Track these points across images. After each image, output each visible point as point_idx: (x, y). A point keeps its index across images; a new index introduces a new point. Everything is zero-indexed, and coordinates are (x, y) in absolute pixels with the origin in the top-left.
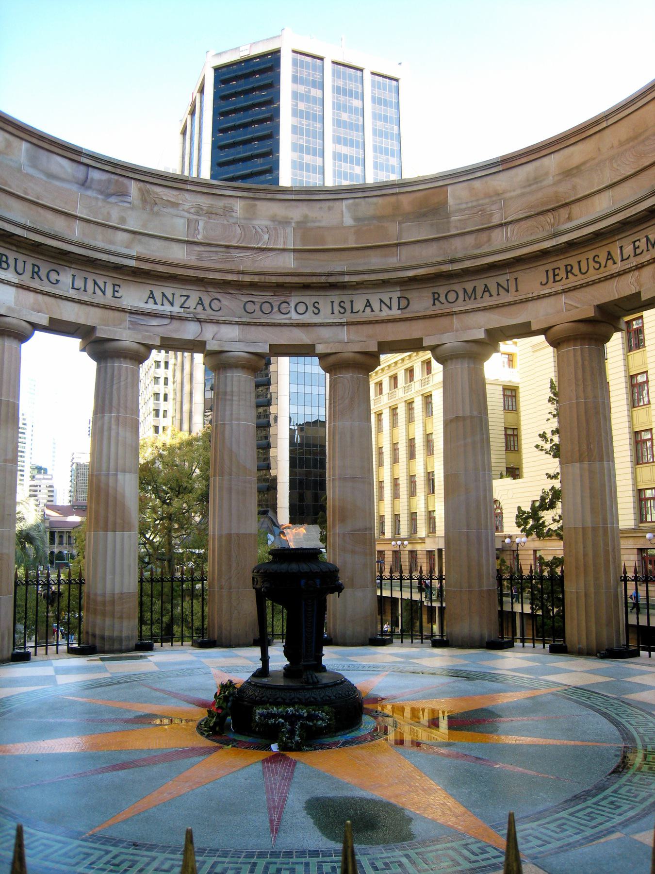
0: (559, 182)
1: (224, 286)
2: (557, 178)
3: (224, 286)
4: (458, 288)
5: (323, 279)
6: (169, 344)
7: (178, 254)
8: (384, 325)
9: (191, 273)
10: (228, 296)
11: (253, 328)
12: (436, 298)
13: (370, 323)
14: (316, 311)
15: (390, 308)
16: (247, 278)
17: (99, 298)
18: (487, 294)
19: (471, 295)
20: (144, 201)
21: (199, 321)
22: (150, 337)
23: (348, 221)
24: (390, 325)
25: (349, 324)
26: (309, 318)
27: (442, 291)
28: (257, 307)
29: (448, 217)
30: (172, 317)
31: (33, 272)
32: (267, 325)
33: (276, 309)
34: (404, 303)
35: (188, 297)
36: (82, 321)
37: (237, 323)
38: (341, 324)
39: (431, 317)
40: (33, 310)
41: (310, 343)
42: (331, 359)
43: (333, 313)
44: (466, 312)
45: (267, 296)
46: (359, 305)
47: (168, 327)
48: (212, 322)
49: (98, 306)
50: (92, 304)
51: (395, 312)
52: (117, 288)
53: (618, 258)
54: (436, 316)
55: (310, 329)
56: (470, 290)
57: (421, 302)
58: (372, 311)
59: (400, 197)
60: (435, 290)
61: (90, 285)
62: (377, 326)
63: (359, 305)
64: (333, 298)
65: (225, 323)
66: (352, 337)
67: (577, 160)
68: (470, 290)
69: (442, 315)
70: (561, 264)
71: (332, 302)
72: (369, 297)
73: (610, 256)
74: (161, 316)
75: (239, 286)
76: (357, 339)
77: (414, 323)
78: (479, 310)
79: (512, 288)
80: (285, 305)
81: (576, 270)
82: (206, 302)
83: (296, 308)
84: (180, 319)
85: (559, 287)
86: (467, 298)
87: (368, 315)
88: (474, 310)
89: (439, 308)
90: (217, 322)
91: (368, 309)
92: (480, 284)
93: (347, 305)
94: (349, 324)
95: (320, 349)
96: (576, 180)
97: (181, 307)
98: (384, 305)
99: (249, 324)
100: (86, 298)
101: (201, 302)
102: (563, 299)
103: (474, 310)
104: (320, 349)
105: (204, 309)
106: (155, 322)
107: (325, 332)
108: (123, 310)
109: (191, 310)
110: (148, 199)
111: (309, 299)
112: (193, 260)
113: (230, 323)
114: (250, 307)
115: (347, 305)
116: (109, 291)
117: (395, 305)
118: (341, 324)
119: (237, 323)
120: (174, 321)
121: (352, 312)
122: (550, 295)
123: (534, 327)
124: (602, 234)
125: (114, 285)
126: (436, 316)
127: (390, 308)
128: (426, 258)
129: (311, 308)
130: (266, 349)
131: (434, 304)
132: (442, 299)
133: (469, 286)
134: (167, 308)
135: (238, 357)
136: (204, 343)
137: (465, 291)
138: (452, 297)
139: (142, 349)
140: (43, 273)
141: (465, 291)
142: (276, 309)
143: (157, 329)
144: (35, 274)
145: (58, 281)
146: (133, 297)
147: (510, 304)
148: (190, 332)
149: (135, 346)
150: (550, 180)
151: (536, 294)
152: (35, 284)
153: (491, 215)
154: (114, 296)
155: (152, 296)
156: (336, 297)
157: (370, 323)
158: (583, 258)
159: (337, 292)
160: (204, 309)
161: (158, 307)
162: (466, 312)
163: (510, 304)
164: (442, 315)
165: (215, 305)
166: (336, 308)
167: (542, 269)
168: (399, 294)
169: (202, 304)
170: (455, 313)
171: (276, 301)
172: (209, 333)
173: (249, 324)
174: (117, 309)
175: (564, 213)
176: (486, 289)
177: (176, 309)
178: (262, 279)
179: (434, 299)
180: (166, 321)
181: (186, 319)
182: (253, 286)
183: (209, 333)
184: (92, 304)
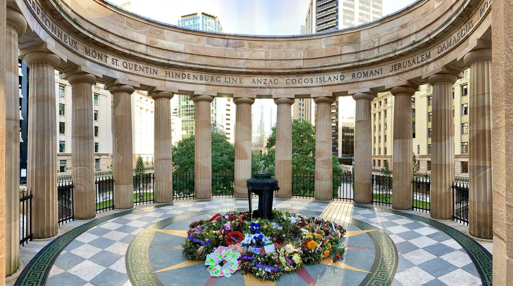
0: (399, 30)
1: (279, 74)
2: (399, 28)
3: (279, 74)
4: (361, 72)
5: (313, 70)
6: (260, 97)
7: (262, 65)
9: (266, 71)
12: (354, 76)
16: (286, 71)
19: (366, 75)
20: (250, 47)
21: (270, 88)
23: (324, 47)
25: (322, 86)
27: (356, 73)
29: (360, 43)
30: (261, 88)
32: (294, 87)
33: (297, 82)
34: (342, 77)
37: (284, 88)
38: (319, 86)
39: (351, 83)
44: (364, 81)
45: (294, 77)
46: (327, 78)
48: (274, 88)
51: (339, 81)
53: (416, 62)
56: (365, 73)
57: (348, 78)
59: (343, 36)
60: (353, 73)
61: (231, 80)
63: (327, 78)
64: (317, 77)
65: (279, 88)
67: (406, 21)
68: (365, 73)
69: (355, 82)
70: (397, 63)
72: (330, 75)
73: (414, 61)
74: (257, 88)
75: (284, 74)
77: (346, 85)
78: (368, 80)
79: (380, 73)
81: (402, 66)
82: (273, 81)
83: (305, 81)
84: (263, 88)
85: (395, 73)
87: (330, 83)
88: (366, 81)
89: (355, 80)
92: (369, 70)
93: (322, 79)
94: (322, 86)
96: (404, 30)
98: (335, 78)
99: (287, 88)
102: (397, 77)
103: (366, 81)
104: (312, 96)
106: (255, 90)
111: (309, 77)
112: (268, 66)
115: (322, 79)
116: (238, 81)
117: (339, 79)
118: (319, 86)
119: (284, 88)
122: (392, 75)
123: (386, 88)
124: (412, 52)
128: (350, 60)
129: (310, 81)
132: (356, 76)
133: (365, 71)
134: (259, 85)
135: (284, 100)
136: (272, 95)
138: (359, 75)
142: (297, 82)
143: (254, 93)
146: (247, 81)
147: (379, 79)
148: (267, 92)
150: (396, 29)
151: (387, 75)
153: (375, 43)
155: (254, 81)
156: (318, 76)
157: (330, 85)
158: (404, 61)
162: (364, 81)
163: (379, 79)
164: (355, 82)
165: (276, 81)
166: (318, 79)
167: (391, 65)
170: (360, 82)
171: (297, 78)
172: (273, 92)
173: (287, 88)
174: (241, 87)
175: (400, 42)
176: (372, 73)
177: (262, 85)
178: (291, 71)
181: (265, 88)
182: (289, 74)
183: (273, 92)
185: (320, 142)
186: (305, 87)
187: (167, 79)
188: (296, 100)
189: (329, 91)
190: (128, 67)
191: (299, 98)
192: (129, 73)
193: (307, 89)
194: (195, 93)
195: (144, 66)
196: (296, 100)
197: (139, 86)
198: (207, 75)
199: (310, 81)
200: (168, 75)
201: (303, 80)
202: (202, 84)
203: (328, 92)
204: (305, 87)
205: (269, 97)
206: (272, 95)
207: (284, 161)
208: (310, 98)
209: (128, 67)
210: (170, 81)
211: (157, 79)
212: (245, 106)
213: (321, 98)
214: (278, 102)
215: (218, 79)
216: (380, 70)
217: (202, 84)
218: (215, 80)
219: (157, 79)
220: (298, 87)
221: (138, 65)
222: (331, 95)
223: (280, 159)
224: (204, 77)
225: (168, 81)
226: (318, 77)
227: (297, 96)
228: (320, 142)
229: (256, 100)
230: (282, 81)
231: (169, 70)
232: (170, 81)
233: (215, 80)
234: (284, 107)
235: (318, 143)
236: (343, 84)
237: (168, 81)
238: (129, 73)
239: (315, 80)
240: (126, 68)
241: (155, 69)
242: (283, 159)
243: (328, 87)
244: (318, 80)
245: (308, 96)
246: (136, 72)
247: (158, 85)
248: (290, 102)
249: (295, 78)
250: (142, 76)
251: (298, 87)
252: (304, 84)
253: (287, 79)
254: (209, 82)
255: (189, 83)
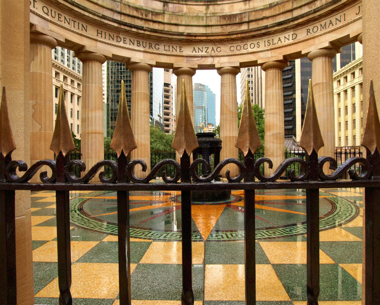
4: (318, 25)
6: (202, 67)
8: (286, 47)
10: (223, 45)
11: (233, 57)
12: (308, 31)
13: (280, 48)
14: (258, 46)
15: (289, 40)
17: (175, 53)
18: (331, 25)
21: (212, 57)
22: (194, 65)
24: (288, 47)
26: (256, 49)
27: (311, 28)
28: (235, 48)
30: (202, 57)
31: (150, 46)
33: (242, 48)
35: (208, 48)
36: (168, 62)
38: (268, 50)
40: (150, 60)
41: (255, 60)
42: (264, 65)
43: (265, 46)
47: (201, 60)
48: (217, 56)
49: (174, 56)
50: (171, 55)
51: (291, 41)
52: (181, 48)
54: (307, 40)
55: (256, 54)
56: (323, 25)
57: (302, 34)
58: (281, 42)
60: (308, 28)
62: (283, 48)
65: (222, 56)
66: (272, 55)
71: (265, 41)
76: (275, 55)
80: (246, 45)
82: (215, 49)
83: (250, 46)
86: (322, 29)
87: (280, 44)
88: (325, 34)
89: (310, 36)
90: (219, 56)
91: (280, 42)
92: (327, 21)
95: (259, 62)
97: (206, 52)
99: (231, 55)
100: (169, 53)
101: (213, 49)
103: (325, 34)
104: (259, 62)
105: (214, 52)
106: (196, 59)
107: (261, 55)
108: (183, 56)
109: (210, 53)
110: (191, 12)
113: (224, 56)
114: (232, 49)
115: (271, 42)
116: (178, 50)
117: (291, 38)
118: (268, 50)
120: (204, 59)
121: (273, 44)
125: (180, 47)
126: (307, 40)
127: (289, 40)
129: (256, 45)
130: (238, 65)
131: (307, 35)
133: (323, 23)
135: (227, 69)
136: (214, 65)
137: (321, 25)
138: (315, 29)
139: (191, 70)
140: (153, 46)
141: (321, 25)
142: (242, 48)
143: (195, 62)
144: (150, 46)
145: (159, 48)
146: (187, 51)
147: (341, 27)
148: (209, 61)
149: (188, 69)
152: (150, 50)
154: (180, 51)
156: (266, 39)
157: (280, 48)
159: (267, 37)
160: (214, 52)
161: (197, 54)
163: (341, 27)
166: (266, 43)
168: (292, 33)
169: (214, 50)
170: (317, 37)
171: (242, 45)
173: (231, 55)
179: (308, 32)
180: (200, 58)
184: (171, 55)
185: (270, 114)
186: (251, 53)
187: (99, 39)
188: (242, 69)
189: (280, 53)
190: (50, 14)
191: (245, 67)
192: (51, 22)
193: (253, 54)
194: (132, 60)
195: (71, 18)
196: (242, 69)
197: (63, 40)
198: (145, 41)
199: (256, 45)
200: (100, 35)
201: (249, 45)
202: (140, 51)
203: (279, 55)
204: (251, 53)
205: (211, 67)
206: (214, 65)
207: (230, 137)
208: (258, 65)
209: (50, 14)
210: (103, 42)
211: (87, 37)
212: (184, 78)
213: (269, 63)
214: (222, 72)
215: (157, 47)
216: (343, 17)
217: (140, 51)
218: (153, 47)
219: (87, 37)
220: (243, 54)
221: (63, 15)
222: (281, 58)
223: (225, 136)
224: (141, 43)
225: (100, 41)
226: (266, 40)
227: (243, 65)
228: (270, 114)
229: (197, 71)
230: (225, 49)
231: (102, 30)
232: (103, 42)
233: (153, 47)
234: (228, 77)
235: (268, 115)
236: (295, 43)
237: (100, 41)
238: (51, 22)
239: (262, 44)
240: (47, 14)
241: (85, 25)
242: (228, 135)
243: (278, 50)
244: (266, 43)
245: (254, 64)
246: (59, 23)
247: (89, 45)
248: (235, 71)
249: (240, 44)
250: (67, 29)
251: (243, 54)
252: (250, 50)
253: (230, 46)
254: (147, 49)
255: (125, 48)
